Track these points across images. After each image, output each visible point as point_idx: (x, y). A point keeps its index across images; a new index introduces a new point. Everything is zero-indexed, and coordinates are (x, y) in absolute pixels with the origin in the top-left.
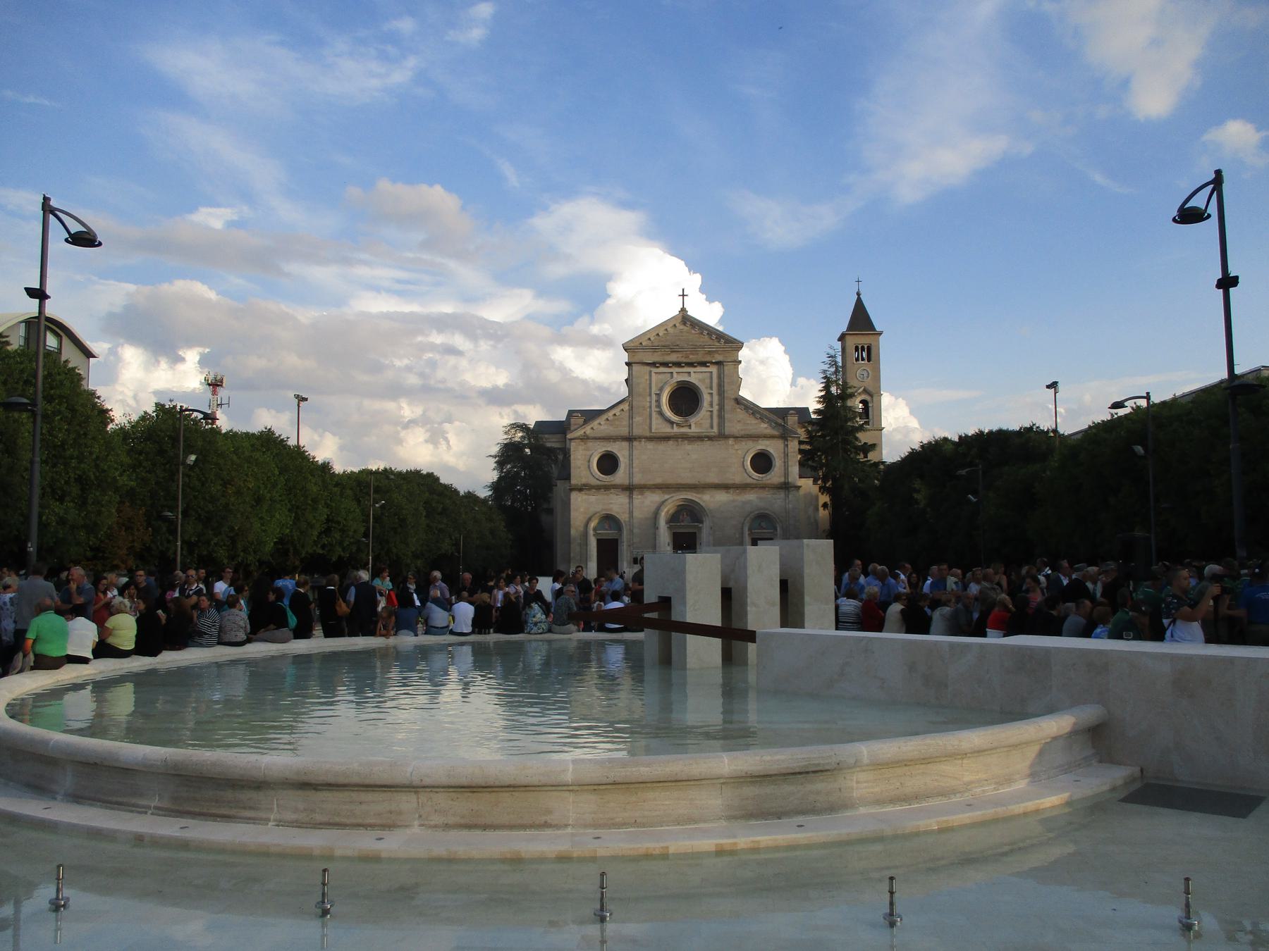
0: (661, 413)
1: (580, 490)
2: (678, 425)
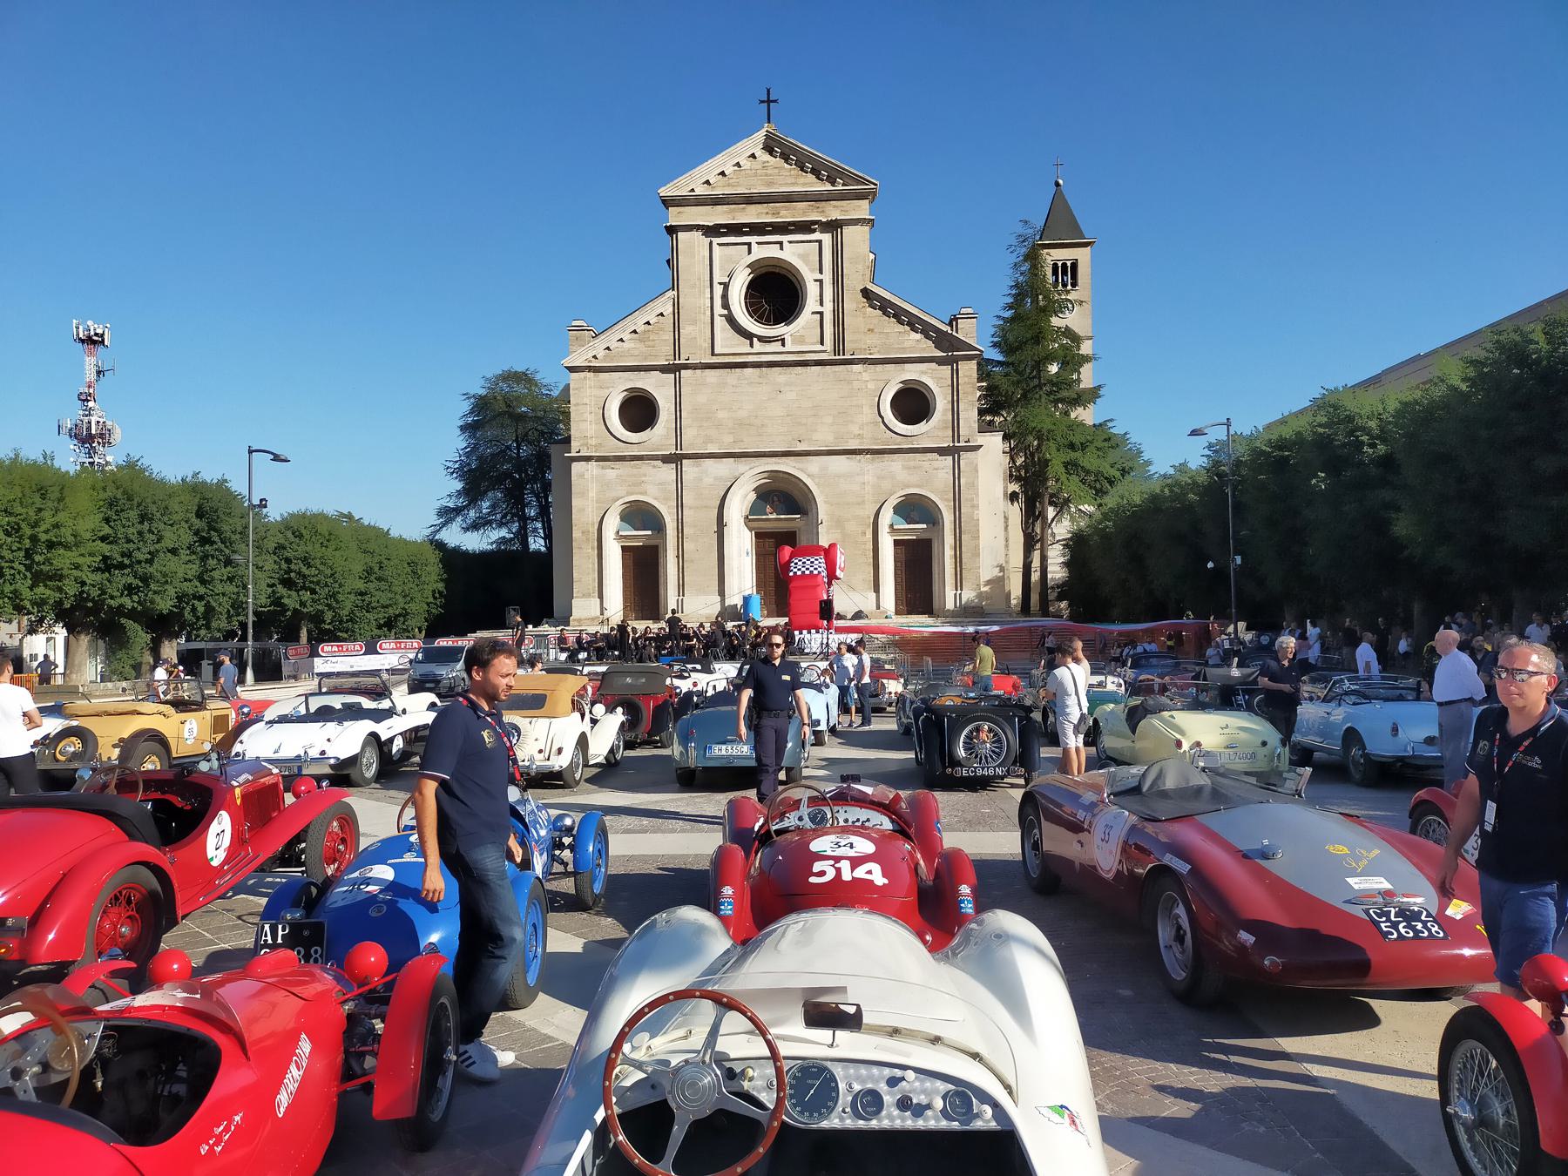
0: (731, 320)
1: (588, 459)
2: (762, 339)
